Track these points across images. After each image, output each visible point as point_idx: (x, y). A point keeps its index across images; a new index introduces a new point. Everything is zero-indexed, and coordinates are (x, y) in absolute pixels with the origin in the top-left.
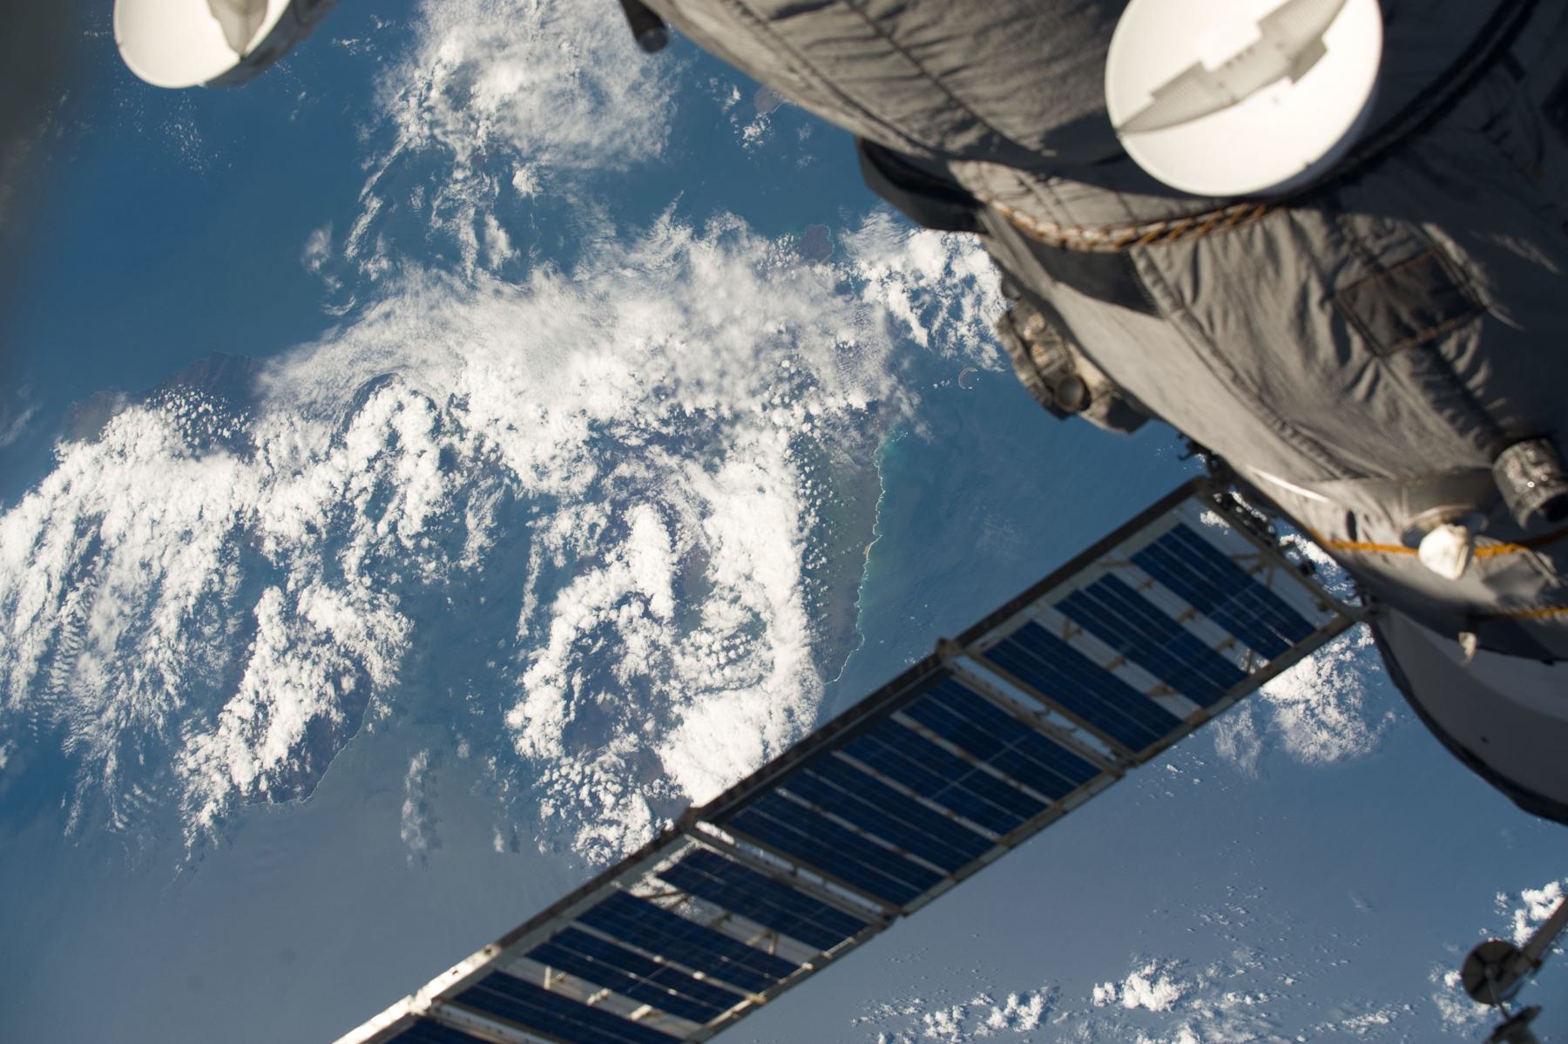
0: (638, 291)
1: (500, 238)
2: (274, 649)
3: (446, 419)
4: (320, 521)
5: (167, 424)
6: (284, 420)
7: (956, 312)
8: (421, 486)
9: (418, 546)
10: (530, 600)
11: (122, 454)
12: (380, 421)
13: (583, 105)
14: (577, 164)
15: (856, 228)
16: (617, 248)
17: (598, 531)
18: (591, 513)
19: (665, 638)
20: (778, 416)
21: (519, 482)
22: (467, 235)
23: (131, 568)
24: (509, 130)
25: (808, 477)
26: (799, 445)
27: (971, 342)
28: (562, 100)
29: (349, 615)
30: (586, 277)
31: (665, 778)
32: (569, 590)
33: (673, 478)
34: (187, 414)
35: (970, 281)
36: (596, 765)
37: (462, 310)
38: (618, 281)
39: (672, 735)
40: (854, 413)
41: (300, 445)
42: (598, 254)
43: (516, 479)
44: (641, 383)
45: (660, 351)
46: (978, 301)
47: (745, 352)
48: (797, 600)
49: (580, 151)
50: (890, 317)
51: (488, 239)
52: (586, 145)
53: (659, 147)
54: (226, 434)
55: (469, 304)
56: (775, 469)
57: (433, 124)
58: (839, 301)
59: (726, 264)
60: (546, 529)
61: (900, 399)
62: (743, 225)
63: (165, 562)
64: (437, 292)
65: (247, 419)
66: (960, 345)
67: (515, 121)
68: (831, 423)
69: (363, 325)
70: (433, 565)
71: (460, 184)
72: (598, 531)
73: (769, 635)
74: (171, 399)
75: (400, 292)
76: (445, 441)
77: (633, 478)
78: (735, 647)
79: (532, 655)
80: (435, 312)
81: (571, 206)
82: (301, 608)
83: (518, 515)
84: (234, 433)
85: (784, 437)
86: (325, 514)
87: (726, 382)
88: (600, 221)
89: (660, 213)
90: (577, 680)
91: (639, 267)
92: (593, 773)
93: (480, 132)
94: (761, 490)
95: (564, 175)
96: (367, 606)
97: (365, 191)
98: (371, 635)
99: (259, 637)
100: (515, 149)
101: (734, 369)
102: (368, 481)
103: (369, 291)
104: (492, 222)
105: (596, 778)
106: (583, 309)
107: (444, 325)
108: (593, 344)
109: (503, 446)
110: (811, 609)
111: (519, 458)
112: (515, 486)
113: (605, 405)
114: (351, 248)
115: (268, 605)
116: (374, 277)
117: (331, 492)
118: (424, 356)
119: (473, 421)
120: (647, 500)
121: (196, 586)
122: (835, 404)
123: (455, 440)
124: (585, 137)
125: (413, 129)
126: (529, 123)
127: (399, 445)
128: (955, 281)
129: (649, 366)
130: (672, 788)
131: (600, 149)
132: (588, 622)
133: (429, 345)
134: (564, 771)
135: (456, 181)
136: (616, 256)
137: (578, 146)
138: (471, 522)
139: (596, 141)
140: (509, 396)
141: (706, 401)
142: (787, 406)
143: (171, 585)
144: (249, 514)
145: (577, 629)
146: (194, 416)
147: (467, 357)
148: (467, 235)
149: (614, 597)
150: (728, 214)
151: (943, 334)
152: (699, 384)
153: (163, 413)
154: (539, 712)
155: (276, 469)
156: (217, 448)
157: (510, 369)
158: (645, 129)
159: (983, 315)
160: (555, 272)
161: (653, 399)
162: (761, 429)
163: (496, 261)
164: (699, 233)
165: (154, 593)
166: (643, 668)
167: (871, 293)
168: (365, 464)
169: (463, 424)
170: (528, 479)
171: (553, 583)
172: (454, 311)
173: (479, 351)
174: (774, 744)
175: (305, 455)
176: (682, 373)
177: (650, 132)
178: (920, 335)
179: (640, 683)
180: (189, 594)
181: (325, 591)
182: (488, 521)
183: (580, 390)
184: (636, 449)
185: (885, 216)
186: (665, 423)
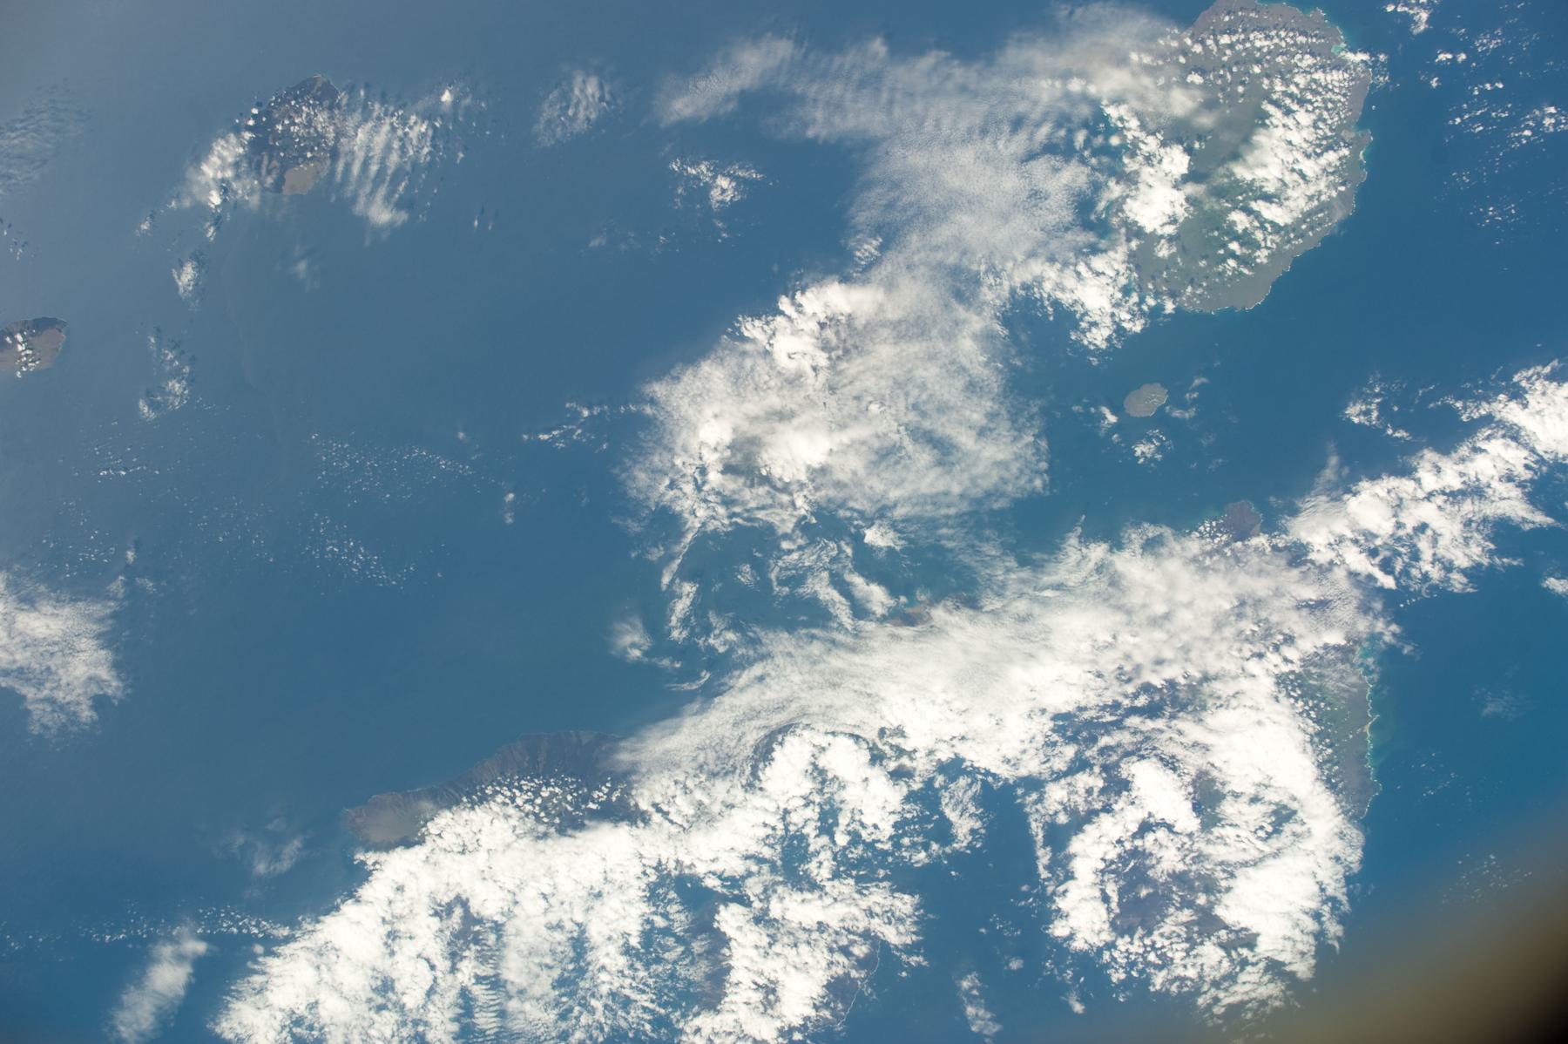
0: (1064, 605)
1: (877, 596)
2: (757, 947)
3: (886, 749)
4: (767, 853)
5: (507, 817)
6: (665, 782)
7: (1415, 556)
8: (876, 805)
9: (897, 845)
10: (1044, 856)
11: (463, 853)
12: (803, 762)
13: (925, 457)
14: (943, 511)
15: (1295, 512)
16: (1025, 574)
17: (1096, 791)
18: (1083, 780)
19: (1200, 845)
20: (1253, 666)
21: (994, 775)
22: (827, 593)
23: (537, 934)
24: (832, 493)
25: (1296, 700)
26: (1281, 680)
27: (1436, 574)
28: (892, 459)
29: (841, 909)
30: (998, 605)
31: (1226, 927)
32: (1081, 836)
33: (1165, 736)
34: (526, 802)
35: (1423, 527)
36: (1156, 936)
37: (857, 659)
38: (1034, 599)
39: (1227, 899)
40: (1337, 648)
41: (706, 801)
42: (1003, 586)
43: (988, 773)
44: (1099, 675)
45: (1109, 646)
46: (1435, 540)
47: (1206, 632)
48: (1320, 787)
49: (935, 500)
50: (1353, 575)
51: (858, 594)
52: (946, 494)
53: (1038, 483)
54: (592, 806)
55: (863, 652)
56: (1270, 707)
57: (727, 502)
58: (1295, 573)
59: (1159, 565)
60: (1040, 800)
61: (1381, 634)
62: (1167, 532)
63: (579, 918)
64: (816, 648)
65: (612, 790)
66: (1426, 577)
67: (839, 485)
68: (1307, 662)
69: (733, 692)
70: (923, 855)
71: (794, 554)
72: (1096, 791)
73: (1300, 815)
74: (497, 792)
75: (763, 657)
76: (892, 765)
77: (1119, 745)
78: (1262, 828)
79: (1061, 889)
80: (822, 666)
81: (951, 551)
82: (776, 910)
83: (1003, 802)
84: (600, 803)
85: (1268, 684)
86: (771, 846)
87: (1193, 655)
88: (993, 558)
89: (1064, 539)
90: (1112, 890)
91: (1059, 587)
92: (1154, 943)
93: (800, 502)
94: (1259, 723)
95: (932, 524)
96: (857, 896)
97: (666, 579)
98: (870, 913)
99: (733, 943)
100: (852, 509)
101: (1199, 644)
102: (812, 813)
103: (723, 667)
104: (858, 580)
105: (1158, 945)
106: (1005, 632)
107: (839, 672)
108: (1031, 656)
109: (962, 755)
110: (1331, 786)
111: (984, 757)
112: (990, 779)
113: (1063, 700)
114: (675, 634)
115: (730, 919)
116: (722, 650)
117: (770, 831)
118: (828, 702)
119: (916, 740)
120: (1142, 757)
121: (634, 928)
122: (1308, 644)
123: (905, 761)
124: (940, 486)
125: (701, 513)
126: (859, 484)
127: (830, 775)
128: (1409, 530)
129: (1102, 661)
130: (1237, 932)
131: (962, 496)
132: (1112, 854)
133: (829, 692)
134: (1123, 949)
135: (790, 552)
136: (1023, 581)
137: (937, 494)
138: (952, 815)
139: (956, 489)
140: (951, 716)
141: (1173, 672)
142: (1260, 656)
143: (596, 932)
144: (672, 865)
145: (1103, 860)
146: (539, 801)
147: (882, 694)
148: (827, 593)
149: (1134, 828)
150: (1146, 525)
151: (1405, 572)
152: (1160, 662)
153: (496, 808)
154: (1082, 916)
155: (686, 825)
156: (592, 824)
157: (944, 696)
158: (1015, 467)
159: (1441, 552)
160: (958, 608)
161: (1115, 682)
162: (1235, 678)
163: (879, 611)
164: (1117, 545)
165: (580, 944)
166: (1180, 867)
167: (1321, 555)
168: (803, 802)
169: (908, 748)
170: (1004, 772)
171: (1058, 837)
172: (838, 661)
173: (893, 687)
174: (1326, 881)
175: (716, 808)
176: (1138, 658)
177: (1021, 471)
178: (1388, 582)
179: (1179, 878)
180: (626, 935)
181: (798, 896)
182: (972, 809)
183: (1033, 695)
184: (1112, 723)
185: (1323, 498)
186: (1136, 696)
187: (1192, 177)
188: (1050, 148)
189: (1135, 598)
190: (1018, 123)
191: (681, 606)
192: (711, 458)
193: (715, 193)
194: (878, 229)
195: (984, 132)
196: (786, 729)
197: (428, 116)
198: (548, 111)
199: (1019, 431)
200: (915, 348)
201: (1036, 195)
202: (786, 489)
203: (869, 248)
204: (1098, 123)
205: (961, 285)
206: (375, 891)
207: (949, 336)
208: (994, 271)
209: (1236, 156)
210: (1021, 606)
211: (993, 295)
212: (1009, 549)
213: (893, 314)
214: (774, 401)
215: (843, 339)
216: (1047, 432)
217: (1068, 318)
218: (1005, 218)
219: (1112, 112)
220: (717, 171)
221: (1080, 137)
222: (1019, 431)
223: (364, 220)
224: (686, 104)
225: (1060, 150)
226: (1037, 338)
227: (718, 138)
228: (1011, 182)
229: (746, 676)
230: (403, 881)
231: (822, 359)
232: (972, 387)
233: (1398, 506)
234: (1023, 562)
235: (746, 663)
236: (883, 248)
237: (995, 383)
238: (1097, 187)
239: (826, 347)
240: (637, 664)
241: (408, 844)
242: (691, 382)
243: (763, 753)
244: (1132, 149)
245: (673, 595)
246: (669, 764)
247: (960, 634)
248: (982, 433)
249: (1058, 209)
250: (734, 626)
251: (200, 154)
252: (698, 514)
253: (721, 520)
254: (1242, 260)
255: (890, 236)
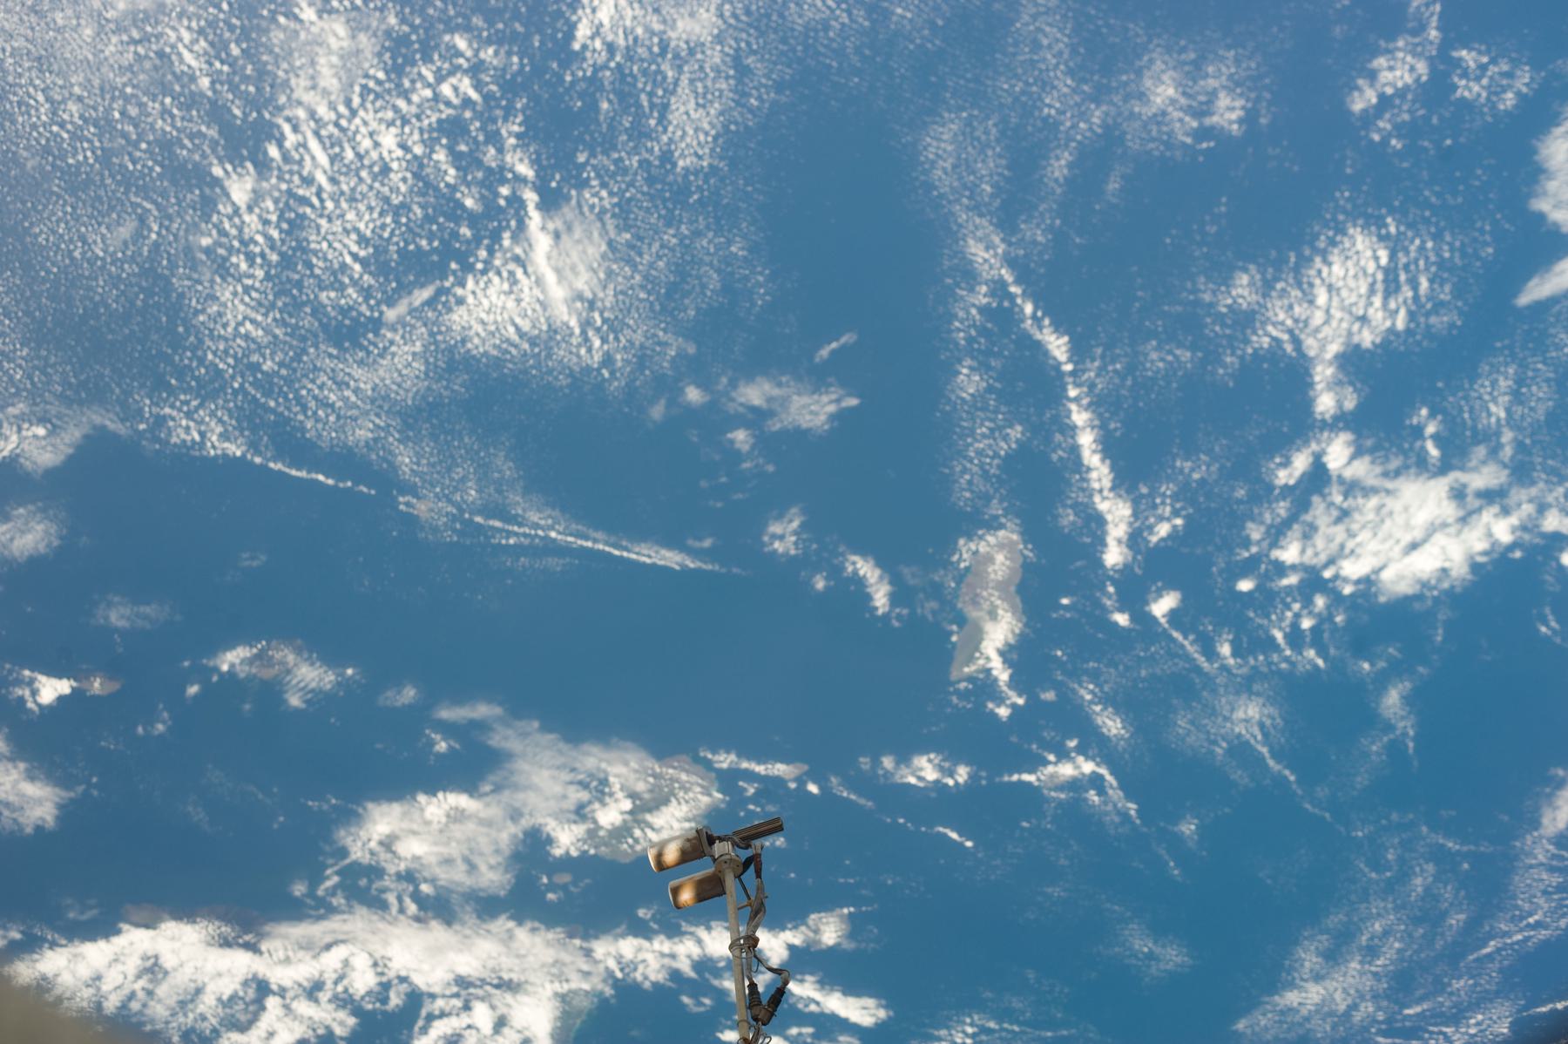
1: (412, 908)
13: (462, 867)
15: (597, 937)
22: (391, 898)
49: (458, 884)
64: (375, 918)
71: (387, 882)
91: (488, 931)
95: (451, 891)
103: (332, 910)
164: (520, 923)
172: (381, 925)
187: (631, 812)
188: (580, 783)
189: (515, 945)
190: (573, 770)
191: (329, 884)
192: (376, 837)
193: (437, 748)
194: (494, 784)
195: (558, 768)
196: (343, 942)
197: (338, 675)
198: (389, 694)
199: (506, 871)
200: (484, 830)
201: (565, 797)
202: (400, 858)
203: (487, 788)
204: (604, 782)
205: (515, 815)
206: (119, 942)
207: (499, 831)
208: (531, 815)
209: (650, 811)
210: (468, 932)
211: (526, 822)
212: (476, 910)
213: (482, 815)
214: (415, 827)
215: (457, 816)
216: (517, 877)
217: (550, 841)
218: (547, 799)
219: (612, 779)
220: (444, 739)
221: (594, 784)
222: (506, 871)
223: (285, 701)
224: (446, 714)
225: (584, 785)
226: (534, 845)
227: (448, 729)
228: (558, 789)
229: (339, 917)
230: (134, 942)
231: (444, 820)
232: (497, 851)
233: (640, 950)
234: (479, 917)
235: (343, 912)
236: (493, 791)
237: (507, 852)
238: (590, 802)
239: (448, 816)
240: (296, 899)
241: (147, 927)
242: (385, 807)
243: (328, 947)
244: (611, 795)
245: (328, 878)
246: (286, 937)
247: (438, 932)
248: (491, 867)
249: (570, 804)
250: (347, 898)
251: (232, 647)
252: (357, 853)
253: (366, 859)
254: (631, 847)
255: (498, 789)
